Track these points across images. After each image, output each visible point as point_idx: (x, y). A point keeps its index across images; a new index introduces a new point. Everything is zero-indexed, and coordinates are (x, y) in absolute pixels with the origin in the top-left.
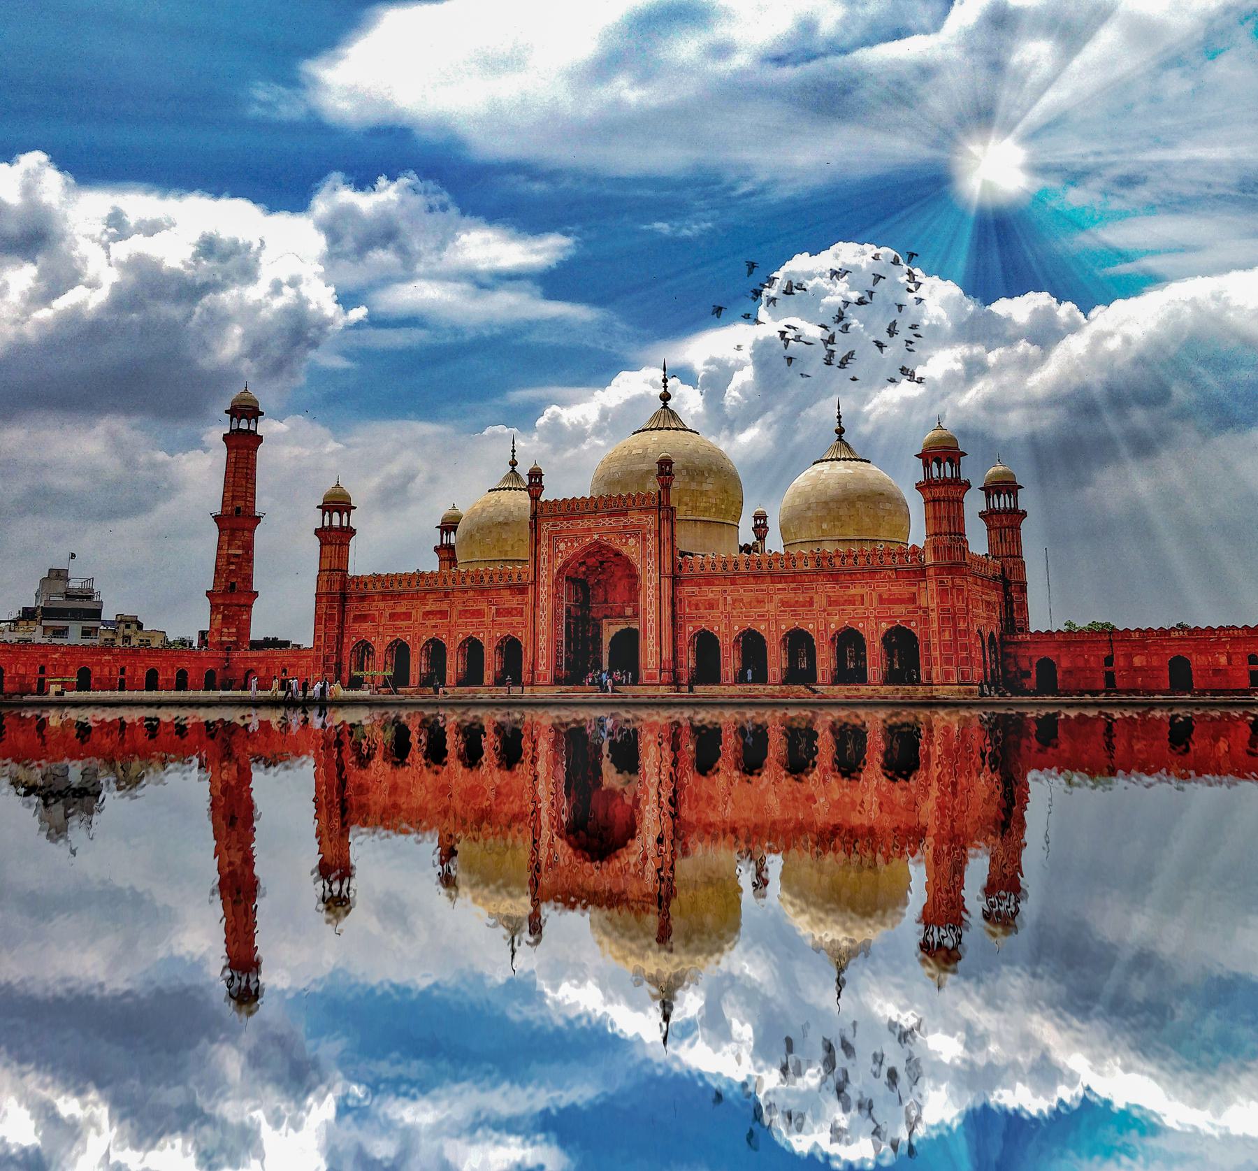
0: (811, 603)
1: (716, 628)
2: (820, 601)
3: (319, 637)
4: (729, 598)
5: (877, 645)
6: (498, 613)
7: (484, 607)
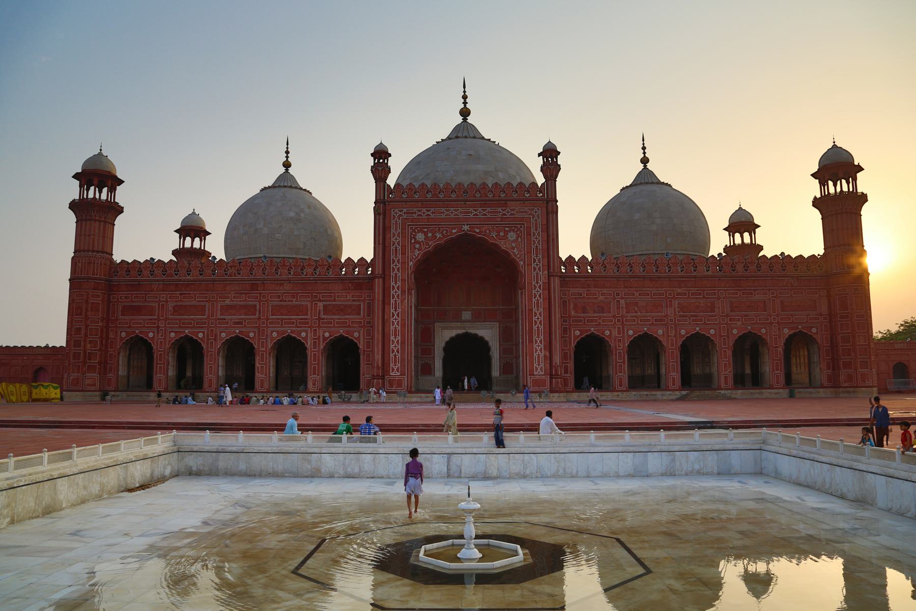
1: (607, 333)
3: (79, 330)
4: (622, 302)
6: (326, 309)
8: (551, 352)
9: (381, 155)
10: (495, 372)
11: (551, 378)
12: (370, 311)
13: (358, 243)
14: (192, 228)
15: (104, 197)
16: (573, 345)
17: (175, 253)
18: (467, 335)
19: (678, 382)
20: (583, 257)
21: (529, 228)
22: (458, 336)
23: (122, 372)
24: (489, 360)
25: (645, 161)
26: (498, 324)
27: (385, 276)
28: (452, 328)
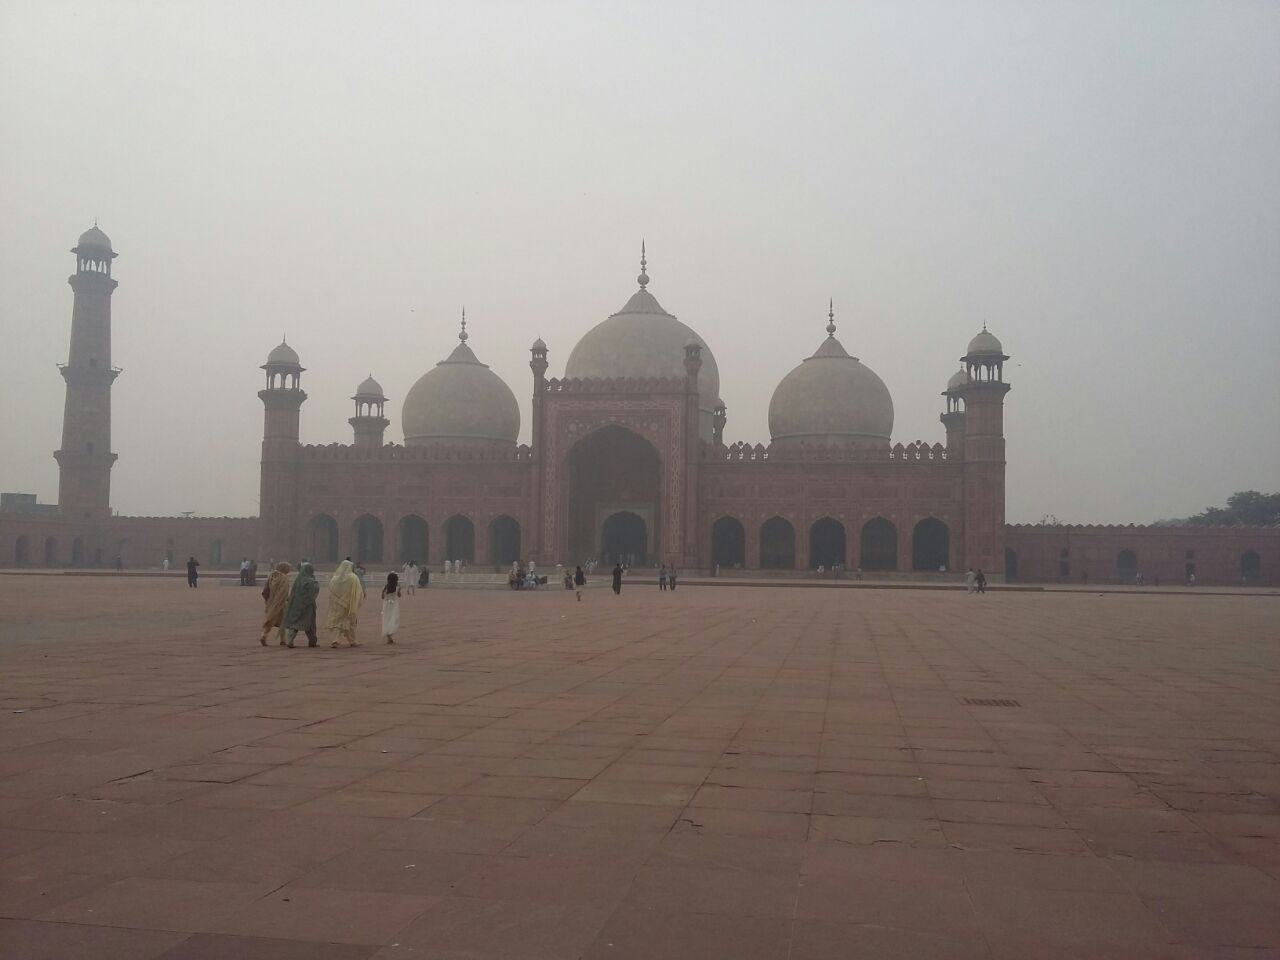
8: (685, 532)
9: (540, 350)
14: (370, 394)
15: (289, 385)
17: (354, 422)
25: (831, 329)
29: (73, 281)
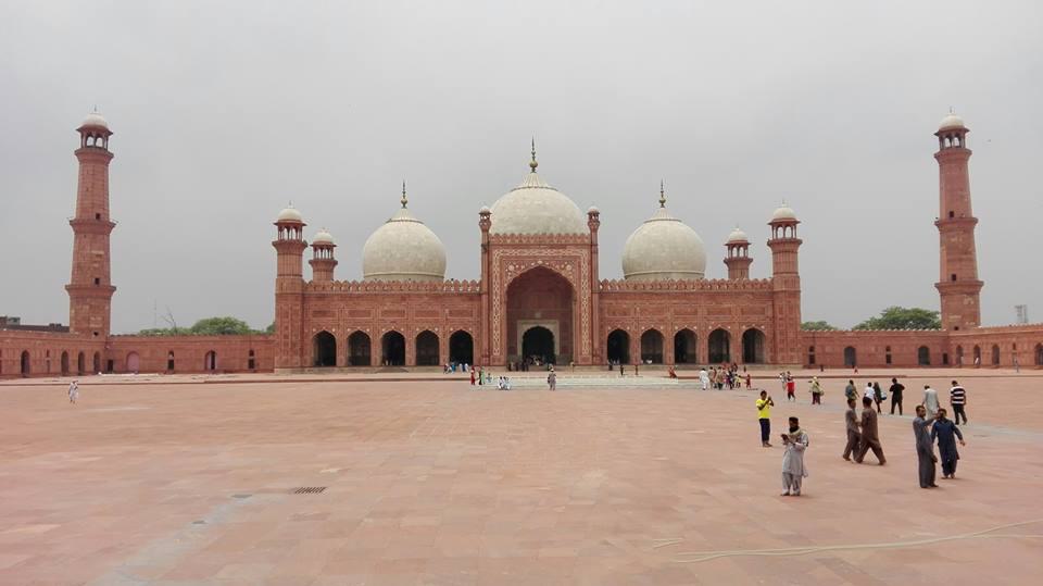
0: (696, 313)
2: (702, 312)
3: (287, 328)
5: (740, 340)
7: (437, 308)
10: (557, 352)
11: (593, 356)
12: (480, 313)
13: (465, 268)
16: (607, 335)
18: (538, 327)
19: (673, 360)
20: (614, 280)
21: (579, 263)
22: (532, 329)
23: (312, 355)
24: (552, 344)
26: (558, 322)
27: (489, 293)
28: (526, 323)
29: (78, 153)
